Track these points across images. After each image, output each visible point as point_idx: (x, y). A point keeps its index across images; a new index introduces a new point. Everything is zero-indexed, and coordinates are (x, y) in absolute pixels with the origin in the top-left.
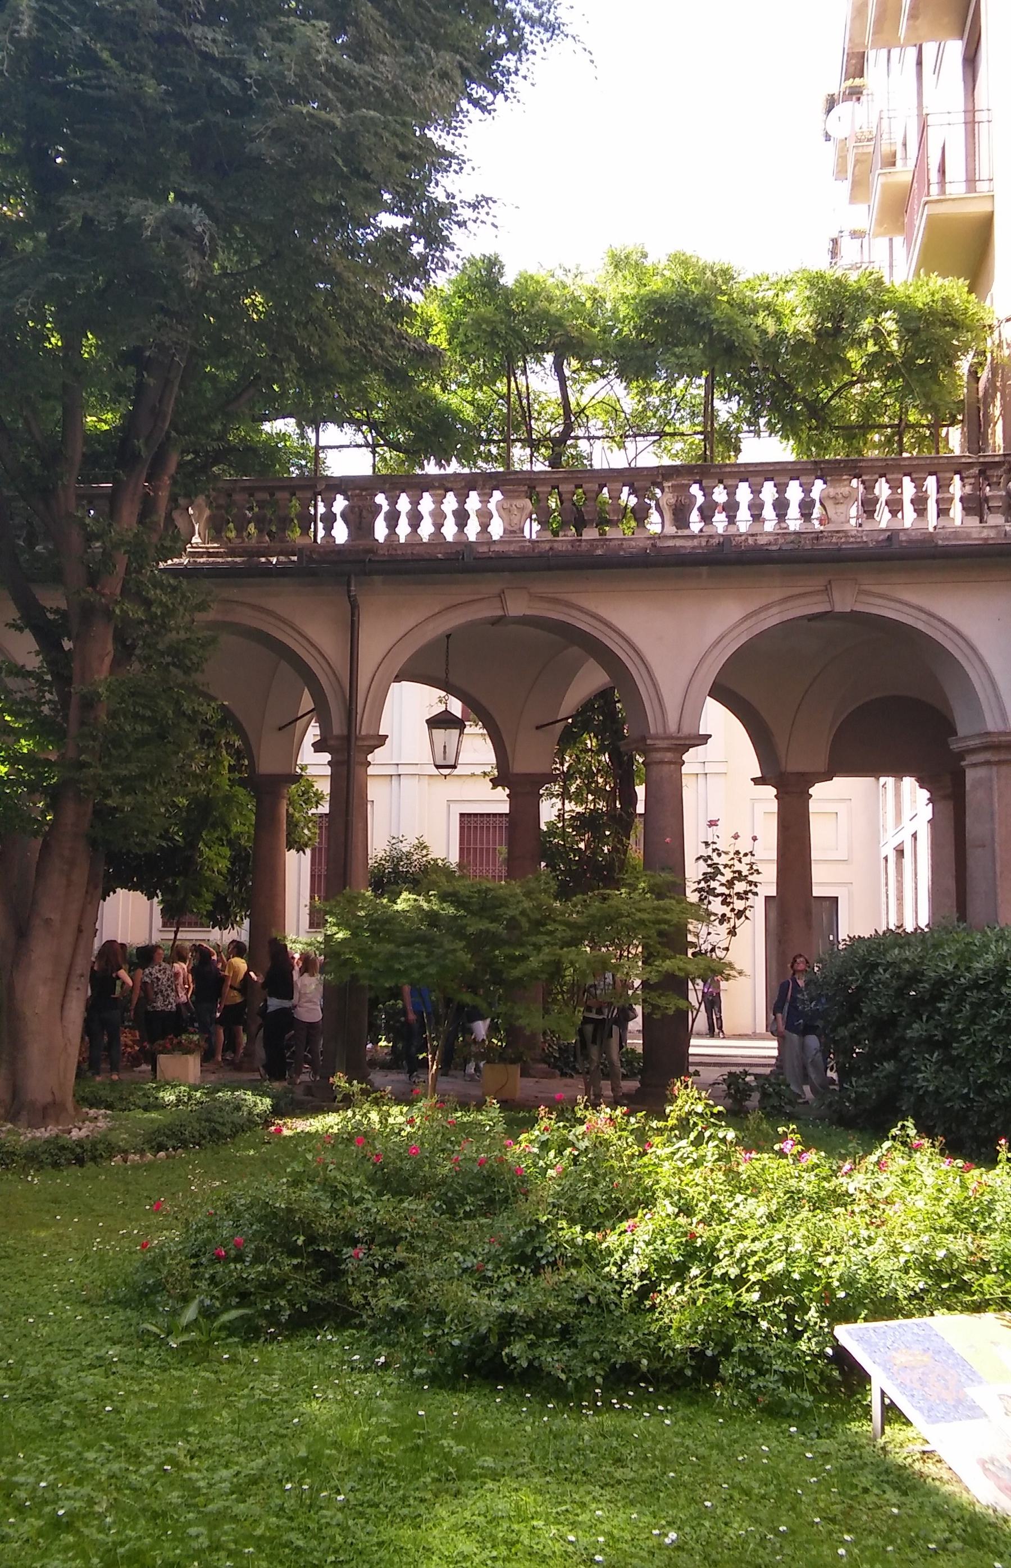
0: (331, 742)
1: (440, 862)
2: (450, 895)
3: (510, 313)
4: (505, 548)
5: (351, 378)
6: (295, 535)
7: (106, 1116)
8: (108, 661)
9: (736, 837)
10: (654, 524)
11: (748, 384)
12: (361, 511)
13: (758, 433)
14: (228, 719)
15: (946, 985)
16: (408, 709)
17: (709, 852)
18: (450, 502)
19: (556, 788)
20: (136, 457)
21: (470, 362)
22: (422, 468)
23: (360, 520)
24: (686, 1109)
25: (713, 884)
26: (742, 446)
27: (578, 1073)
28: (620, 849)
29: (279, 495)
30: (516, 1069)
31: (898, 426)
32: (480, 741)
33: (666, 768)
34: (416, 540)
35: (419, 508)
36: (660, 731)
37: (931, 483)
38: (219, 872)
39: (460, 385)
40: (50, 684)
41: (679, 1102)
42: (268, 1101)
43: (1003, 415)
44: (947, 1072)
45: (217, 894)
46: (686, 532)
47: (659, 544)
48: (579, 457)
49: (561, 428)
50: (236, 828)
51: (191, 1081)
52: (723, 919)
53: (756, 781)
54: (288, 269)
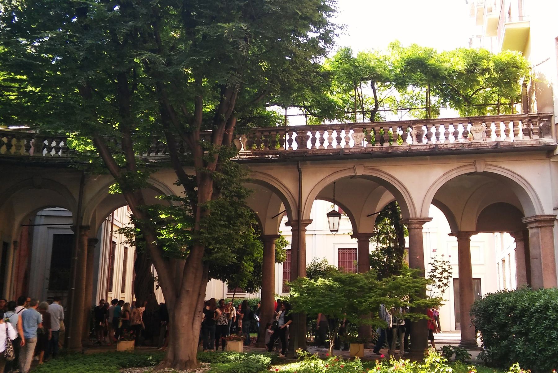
0: (292, 223)
1: (332, 267)
2: (338, 278)
3: (356, 67)
4: (355, 150)
5: (300, 90)
6: (278, 147)
7: (208, 365)
8: (211, 194)
9: (443, 256)
10: (410, 141)
11: (442, 90)
12: (302, 138)
13: (445, 107)
14: (254, 216)
15: (525, 311)
16: (320, 209)
17: (433, 261)
18: (335, 134)
19: (375, 239)
20: (222, 120)
21: (341, 84)
22: (324, 122)
23: (302, 141)
24: (433, 360)
25: (435, 274)
26: (440, 112)
27: (385, 347)
28: (399, 261)
29: (272, 133)
30: (362, 345)
31: (497, 104)
32: (346, 221)
33: (416, 230)
34: (322, 148)
35: (323, 136)
36: (414, 217)
37: (511, 124)
38: (250, 272)
39: (337, 92)
40: (189, 203)
41: (430, 357)
42: (269, 359)
43: (537, 99)
44: (527, 345)
45: (249, 280)
46: (421, 144)
47: (412, 148)
48: (381, 118)
49: (374, 107)
50: (256, 255)
51: (240, 351)
52: (439, 286)
53: (449, 235)
54: (274, 52)
